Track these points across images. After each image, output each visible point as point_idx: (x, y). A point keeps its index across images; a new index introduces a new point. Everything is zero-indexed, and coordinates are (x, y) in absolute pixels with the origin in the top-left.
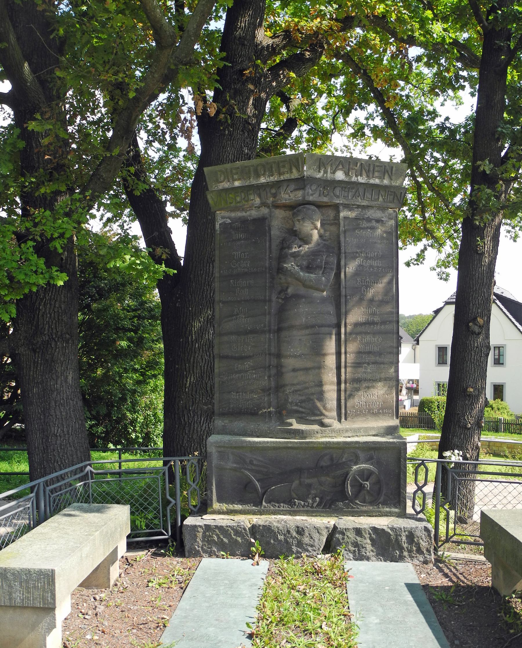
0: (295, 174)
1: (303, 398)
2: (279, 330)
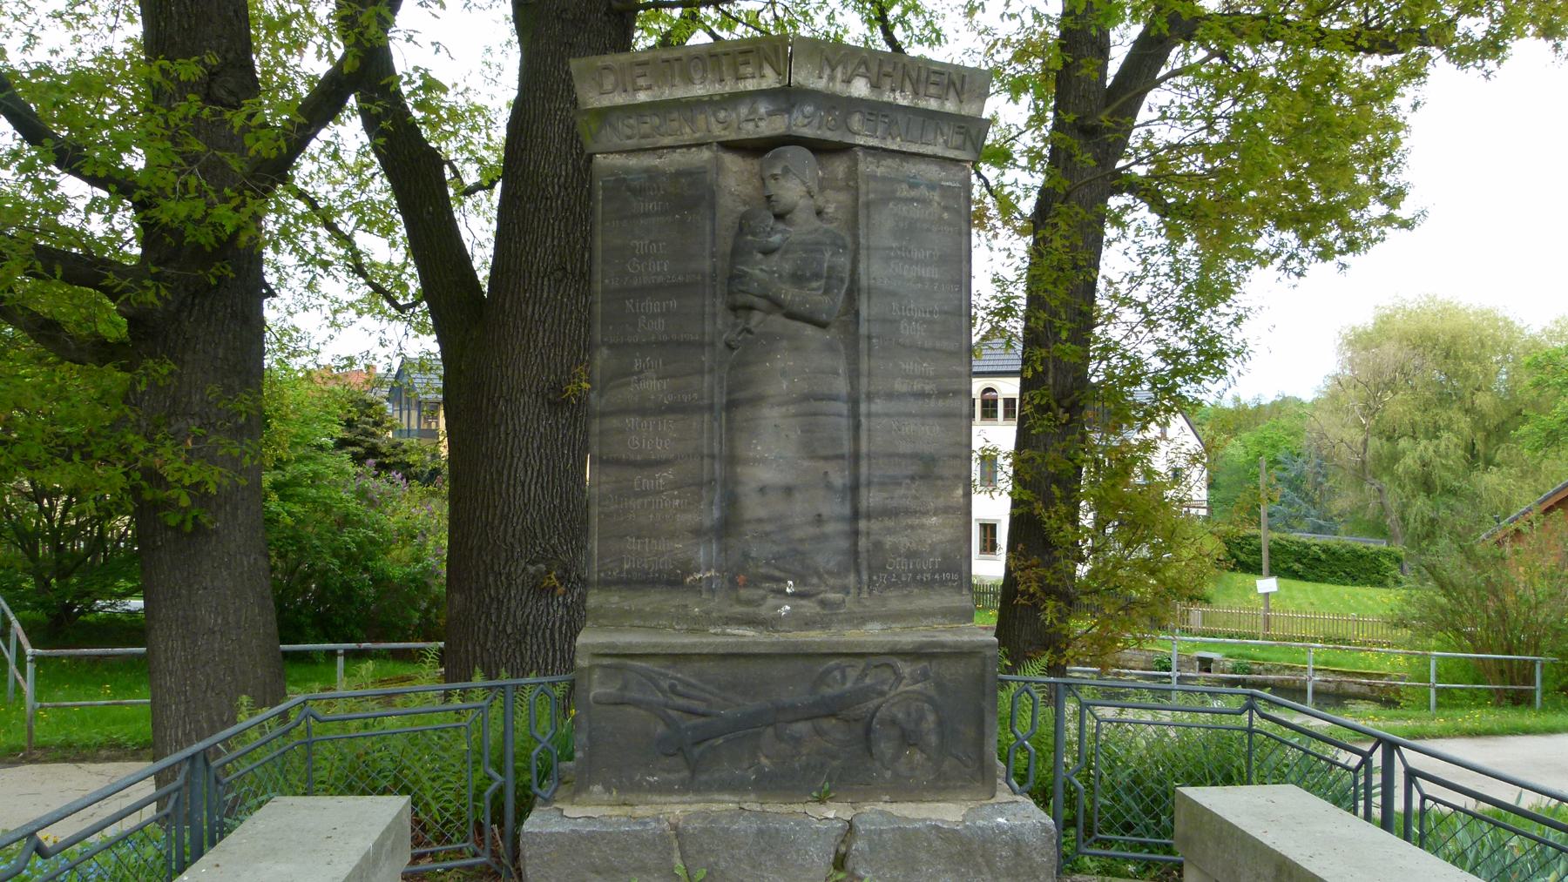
0: (770, 80)
1: (782, 549)
2: (731, 405)
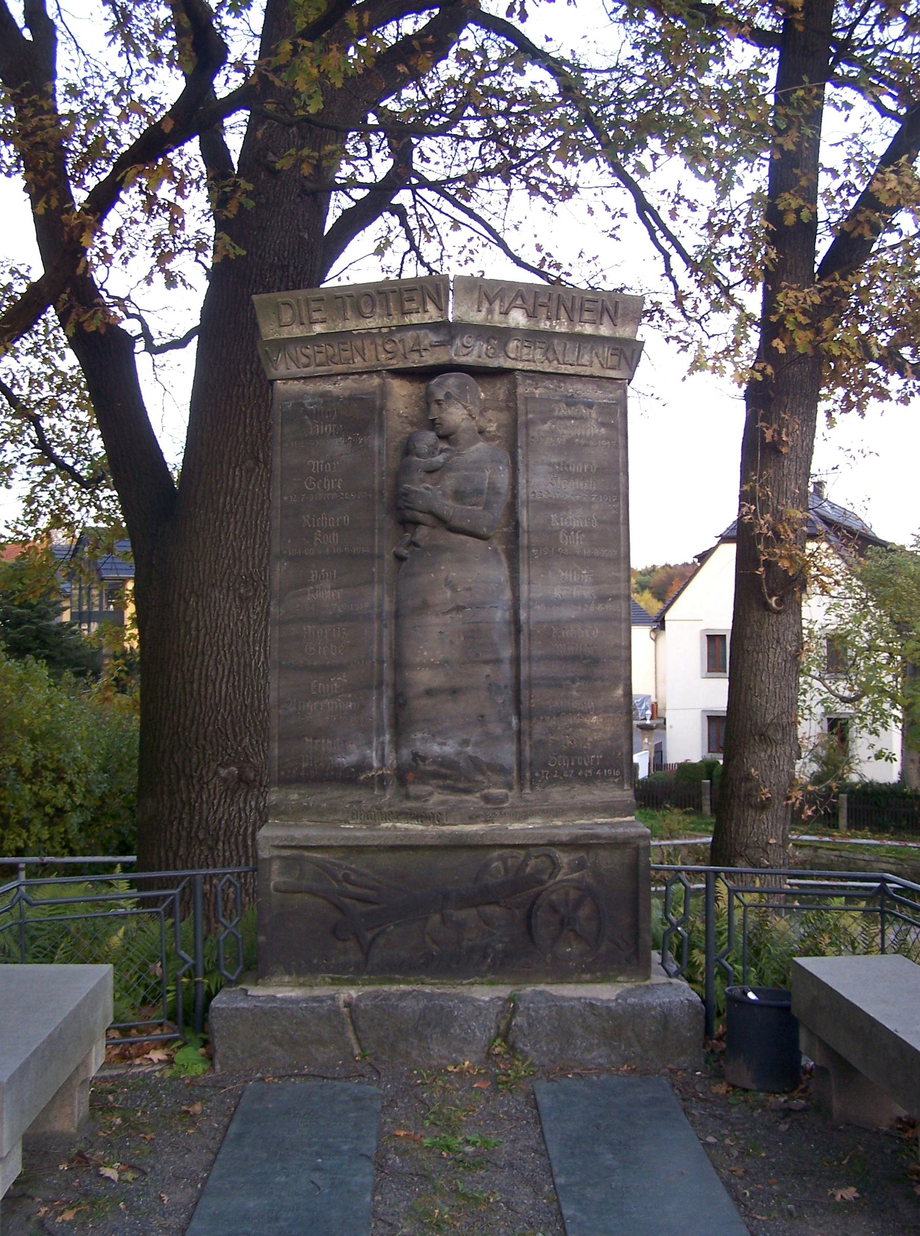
0: (432, 314)
